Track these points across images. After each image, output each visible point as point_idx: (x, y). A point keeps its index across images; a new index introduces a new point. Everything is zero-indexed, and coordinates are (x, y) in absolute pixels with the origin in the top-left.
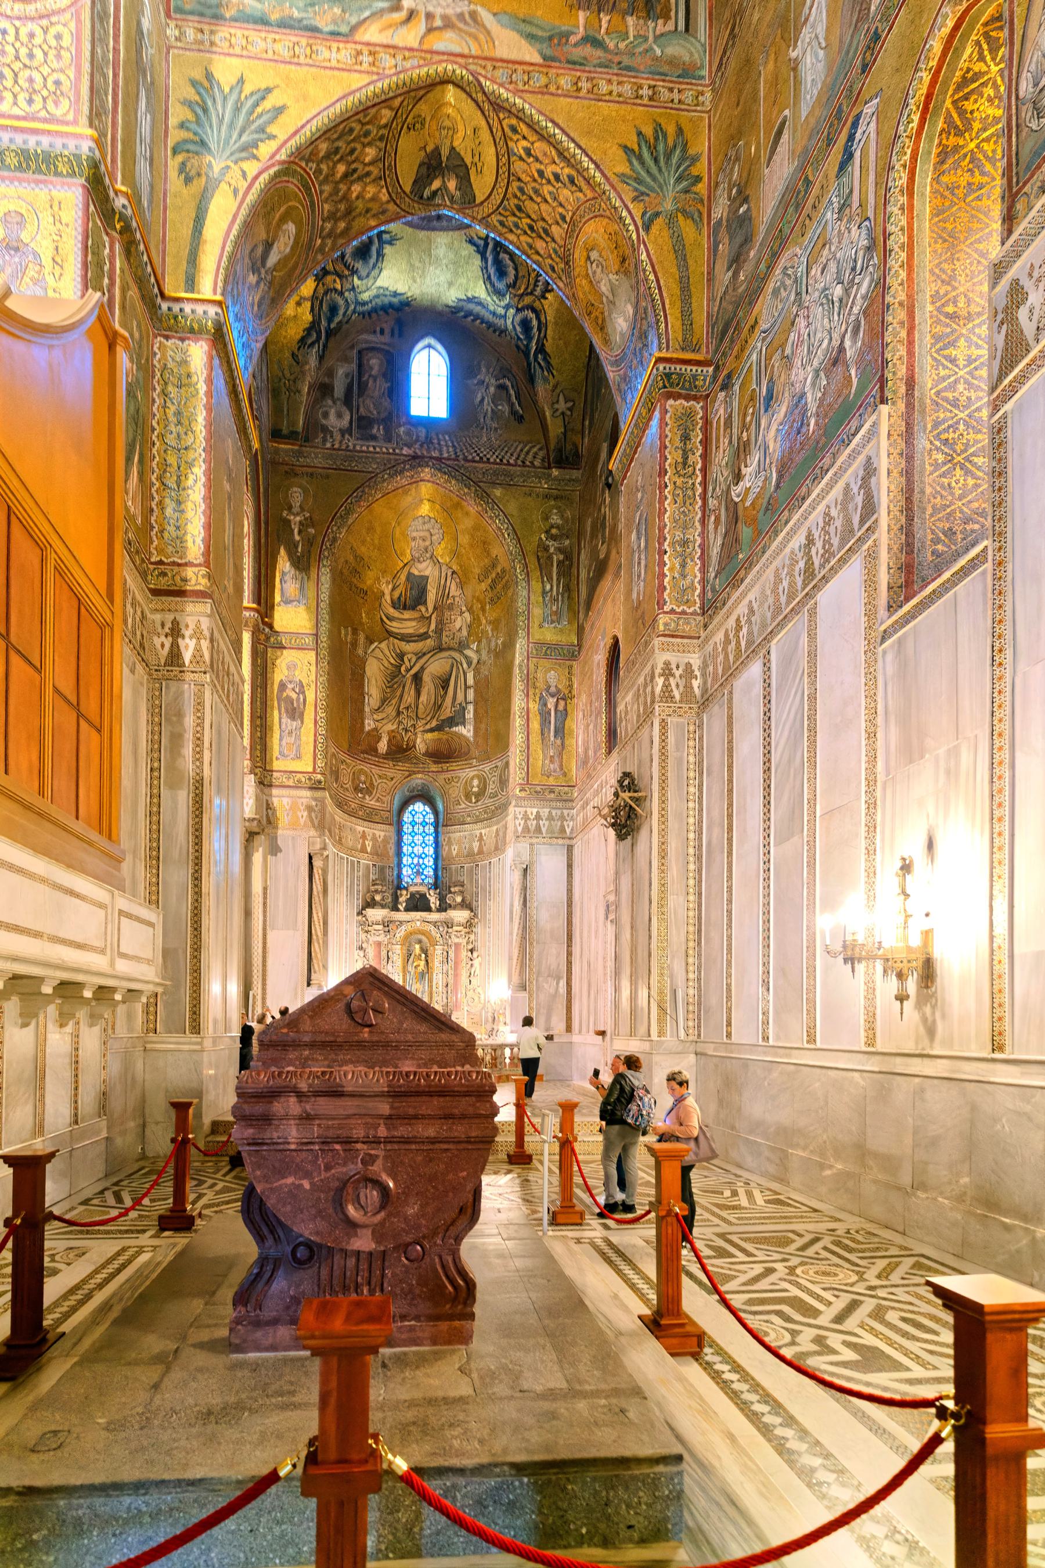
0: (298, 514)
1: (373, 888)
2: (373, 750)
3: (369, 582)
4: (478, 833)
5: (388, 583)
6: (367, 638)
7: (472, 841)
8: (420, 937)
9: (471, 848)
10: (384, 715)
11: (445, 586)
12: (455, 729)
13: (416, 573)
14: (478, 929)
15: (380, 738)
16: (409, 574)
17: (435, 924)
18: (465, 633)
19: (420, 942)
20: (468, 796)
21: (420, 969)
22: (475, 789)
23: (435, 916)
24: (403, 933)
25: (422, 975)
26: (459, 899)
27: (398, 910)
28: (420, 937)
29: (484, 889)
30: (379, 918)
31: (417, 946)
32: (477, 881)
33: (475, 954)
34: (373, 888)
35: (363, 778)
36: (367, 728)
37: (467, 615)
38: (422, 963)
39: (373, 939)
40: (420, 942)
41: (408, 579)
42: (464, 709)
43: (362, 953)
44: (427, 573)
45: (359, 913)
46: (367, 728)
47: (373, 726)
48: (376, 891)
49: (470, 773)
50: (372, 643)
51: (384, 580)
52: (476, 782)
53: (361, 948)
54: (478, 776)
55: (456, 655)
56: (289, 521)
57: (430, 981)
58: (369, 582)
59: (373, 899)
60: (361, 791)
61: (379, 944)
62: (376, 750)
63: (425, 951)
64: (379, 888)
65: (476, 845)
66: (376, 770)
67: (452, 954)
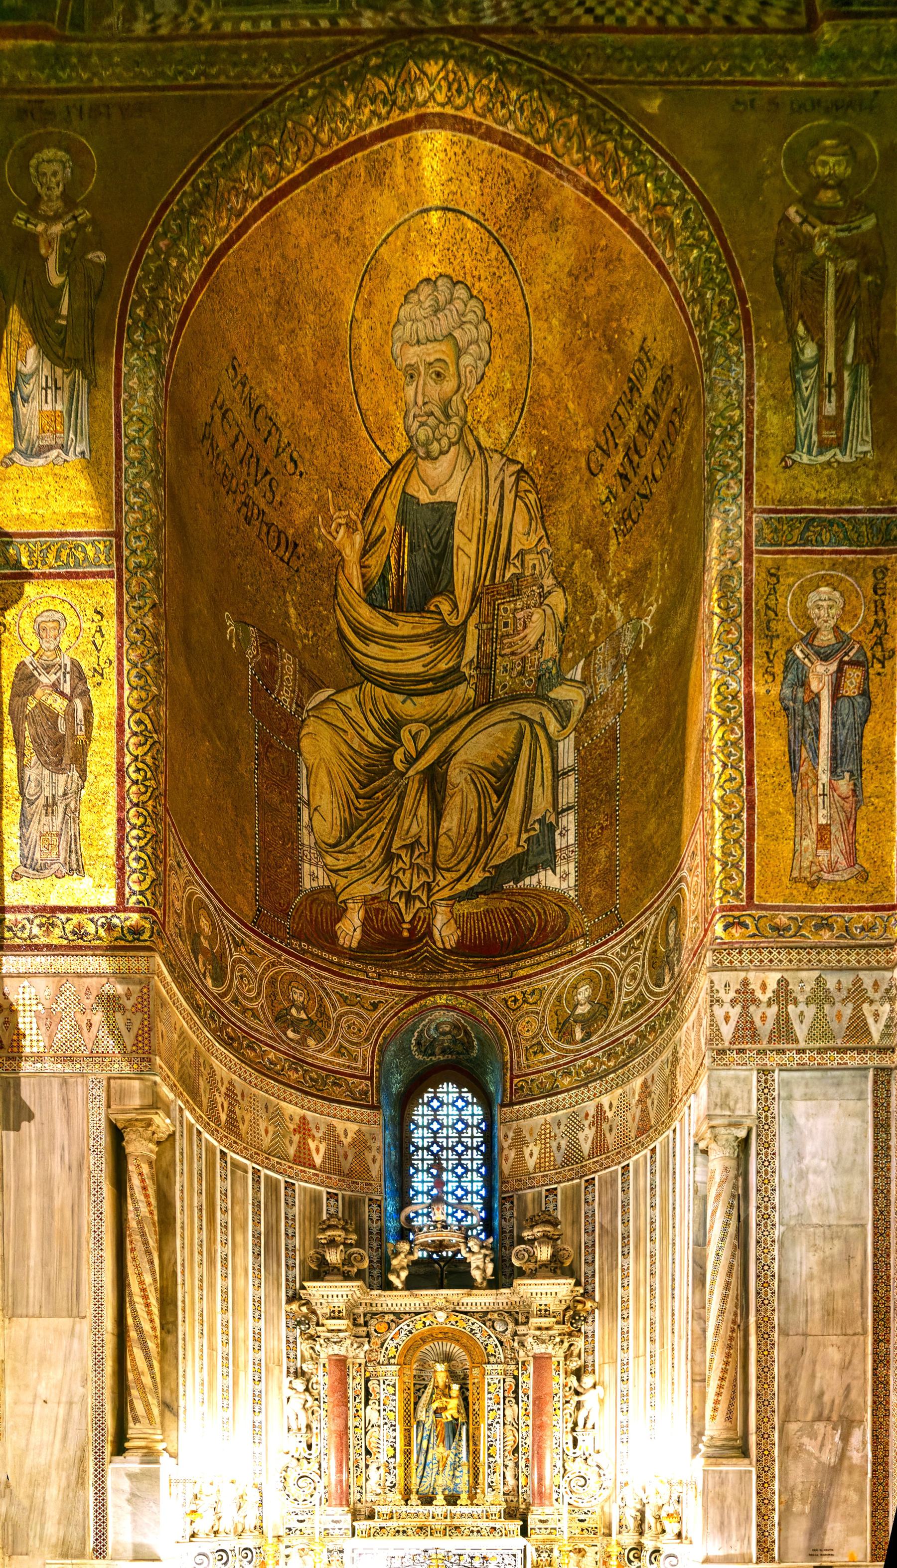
0: (57, 218)
1: (323, 1237)
2: (329, 940)
3: (301, 515)
4: (590, 1107)
5: (351, 528)
6: (302, 670)
7: (575, 1124)
8: (455, 1349)
9: (574, 1145)
10: (353, 860)
11: (498, 526)
12: (530, 881)
13: (425, 497)
14: (597, 1325)
15: (341, 913)
16: (407, 500)
17: (484, 1316)
18: (551, 649)
19: (447, 1358)
20: (564, 1030)
21: (447, 1416)
22: (583, 1009)
23: (482, 1299)
24: (402, 1339)
25: (454, 1428)
26: (544, 1253)
27: (388, 1286)
28: (455, 1349)
29: (608, 1233)
30: (340, 1304)
31: (441, 1368)
32: (590, 1217)
33: (588, 1381)
34: (323, 1237)
35: (298, 997)
36: (307, 884)
37: (558, 601)
38: (453, 1404)
39: (326, 1352)
40: (447, 1358)
41: (403, 516)
42: (552, 828)
43: (299, 1384)
44: (450, 494)
45: (292, 1298)
46: (307, 884)
47: (323, 880)
48: (332, 1243)
49: (571, 973)
50: (317, 686)
51: (340, 518)
52: (584, 992)
53: (299, 1373)
54: (590, 978)
55: (529, 709)
56: (34, 238)
57: (473, 1440)
58: (301, 515)
59: (322, 1261)
60: (295, 1024)
61: (341, 1363)
62: (333, 937)
63: (459, 1377)
64: (340, 1235)
65: (586, 1137)
66: (332, 983)
67: (527, 1381)
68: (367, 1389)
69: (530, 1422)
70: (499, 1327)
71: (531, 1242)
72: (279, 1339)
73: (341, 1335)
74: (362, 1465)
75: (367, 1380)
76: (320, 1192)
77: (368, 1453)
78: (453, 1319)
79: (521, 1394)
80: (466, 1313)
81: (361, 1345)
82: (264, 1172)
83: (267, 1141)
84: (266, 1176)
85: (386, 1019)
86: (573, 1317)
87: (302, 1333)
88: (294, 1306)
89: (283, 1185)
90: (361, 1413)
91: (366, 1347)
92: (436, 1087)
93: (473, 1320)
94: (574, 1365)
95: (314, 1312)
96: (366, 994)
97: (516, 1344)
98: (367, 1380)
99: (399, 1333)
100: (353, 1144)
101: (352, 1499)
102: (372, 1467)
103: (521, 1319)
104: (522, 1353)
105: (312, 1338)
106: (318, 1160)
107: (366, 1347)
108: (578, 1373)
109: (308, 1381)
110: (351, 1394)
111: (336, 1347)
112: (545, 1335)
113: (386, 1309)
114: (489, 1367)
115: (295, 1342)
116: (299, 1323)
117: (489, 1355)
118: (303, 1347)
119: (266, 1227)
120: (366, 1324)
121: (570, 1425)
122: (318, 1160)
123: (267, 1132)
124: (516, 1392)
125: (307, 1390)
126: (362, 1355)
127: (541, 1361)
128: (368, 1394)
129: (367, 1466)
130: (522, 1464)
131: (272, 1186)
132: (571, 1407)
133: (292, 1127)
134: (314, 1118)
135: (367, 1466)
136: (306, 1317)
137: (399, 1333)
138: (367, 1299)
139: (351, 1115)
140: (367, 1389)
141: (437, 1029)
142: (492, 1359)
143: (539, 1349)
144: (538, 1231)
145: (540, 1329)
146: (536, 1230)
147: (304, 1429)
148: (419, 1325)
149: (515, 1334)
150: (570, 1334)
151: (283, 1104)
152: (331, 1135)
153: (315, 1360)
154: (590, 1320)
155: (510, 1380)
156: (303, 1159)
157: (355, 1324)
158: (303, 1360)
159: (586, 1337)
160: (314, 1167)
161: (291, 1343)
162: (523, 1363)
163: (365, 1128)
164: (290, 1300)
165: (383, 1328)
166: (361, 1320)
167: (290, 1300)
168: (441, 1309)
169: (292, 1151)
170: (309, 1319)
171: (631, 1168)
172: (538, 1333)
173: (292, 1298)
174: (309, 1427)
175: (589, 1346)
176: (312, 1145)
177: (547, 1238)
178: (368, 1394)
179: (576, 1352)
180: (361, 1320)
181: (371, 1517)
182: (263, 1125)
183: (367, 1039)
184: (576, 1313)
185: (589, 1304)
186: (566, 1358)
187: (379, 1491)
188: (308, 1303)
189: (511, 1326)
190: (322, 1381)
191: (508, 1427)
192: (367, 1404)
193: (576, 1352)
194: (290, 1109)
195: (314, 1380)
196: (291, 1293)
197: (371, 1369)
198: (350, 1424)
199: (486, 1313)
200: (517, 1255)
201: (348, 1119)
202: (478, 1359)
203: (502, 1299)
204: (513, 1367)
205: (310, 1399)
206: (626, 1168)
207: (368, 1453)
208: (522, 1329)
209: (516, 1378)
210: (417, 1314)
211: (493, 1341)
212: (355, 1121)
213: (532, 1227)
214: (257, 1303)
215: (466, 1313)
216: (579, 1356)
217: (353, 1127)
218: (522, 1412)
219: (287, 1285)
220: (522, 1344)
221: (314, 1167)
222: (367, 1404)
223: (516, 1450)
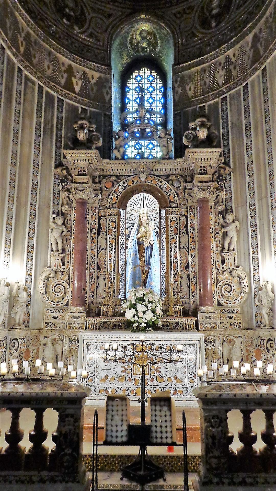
26: (203, 134)
68: (99, 224)
69: (197, 247)
70: (176, 184)
71: (195, 129)
72: (49, 190)
73: (85, 185)
74: (95, 276)
75: (99, 219)
76: (77, 107)
77: (99, 268)
78: (150, 179)
79: (189, 228)
80: (156, 176)
81: (96, 195)
82: (46, 89)
83: (49, 72)
84: (47, 93)
85: (114, 22)
86: (218, 178)
87: (63, 188)
88: (59, 170)
89: (56, 100)
90: (96, 240)
91: (100, 196)
92: (139, 70)
93: (161, 180)
94: (221, 208)
95: (70, 175)
96: (105, 9)
97: (186, 195)
98: (99, 219)
99: (118, 188)
100: (96, 84)
101: (87, 302)
102: (101, 278)
103: (188, 179)
104: (189, 201)
105: (68, 190)
106: (77, 89)
107: (100, 196)
108: (224, 213)
109: (65, 219)
110: (89, 226)
111: (81, 193)
112: (205, 185)
113: (111, 173)
114: (171, 209)
115: (58, 194)
116: (62, 181)
117: (170, 202)
118: (63, 195)
119: (45, 121)
120: (100, 182)
121: (219, 249)
122: (77, 89)
123: (49, 68)
124: (187, 226)
125: (63, 224)
126: (97, 202)
127: (203, 202)
128: (100, 228)
129: (98, 278)
130: (191, 276)
131: (50, 98)
132: (220, 236)
133: (63, 69)
134: (76, 67)
135: (98, 278)
136: (65, 177)
137: (118, 188)
138: (100, 166)
139: (96, 68)
140: (99, 224)
141: (140, 34)
142: (172, 204)
143: (201, 195)
144: (198, 121)
145: (201, 182)
146: (197, 121)
147: (60, 251)
148: (130, 183)
149: (185, 188)
150: (217, 189)
151: (58, 55)
152: (85, 77)
153: (70, 205)
154: (228, 179)
155: (183, 219)
156: (69, 86)
157: (94, 182)
158: (63, 204)
159: (226, 191)
160: (74, 92)
161: (56, 194)
162: (190, 207)
163: (102, 75)
164: (56, 167)
165: (109, 185)
166: (97, 180)
167: (56, 167)
168: (143, 172)
169: (63, 81)
170: (68, 179)
171: (249, 86)
172: (200, 184)
173: (59, 165)
174: (63, 250)
175: (228, 197)
176: (74, 81)
177: (203, 125)
178: (100, 228)
179: (220, 201)
180: (97, 180)
181: (98, 314)
182: (46, 63)
183: (105, 31)
184: (220, 175)
185: (228, 169)
186: (215, 205)
187: (105, 295)
188: (67, 169)
189: (183, 184)
190: (73, 217)
191: (183, 250)
192: (99, 235)
193: (220, 201)
194: (63, 59)
195: (68, 218)
196: (57, 162)
197: (102, 211)
198: (89, 248)
199: (168, 176)
200: (186, 137)
201: (94, 70)
202: (164, 205)
203: (178, 166)
204: (184, 210)
205: (65, 230)
206: (246, 87)
207: (99, 268)
208: (189, 185)
209: (186, 217)
210: (129, 176)
211: (173, 193)
212: (98, 71)
213: (194, 121)
214: (36, 165)
215: (156, 176)
216: (222, 202)
217: (97, 75)
218: (190, 240)
219: (56, 158)
220: (189, 195)
221: (74, 92)
222: (99, 235)
223: (187, 267)
